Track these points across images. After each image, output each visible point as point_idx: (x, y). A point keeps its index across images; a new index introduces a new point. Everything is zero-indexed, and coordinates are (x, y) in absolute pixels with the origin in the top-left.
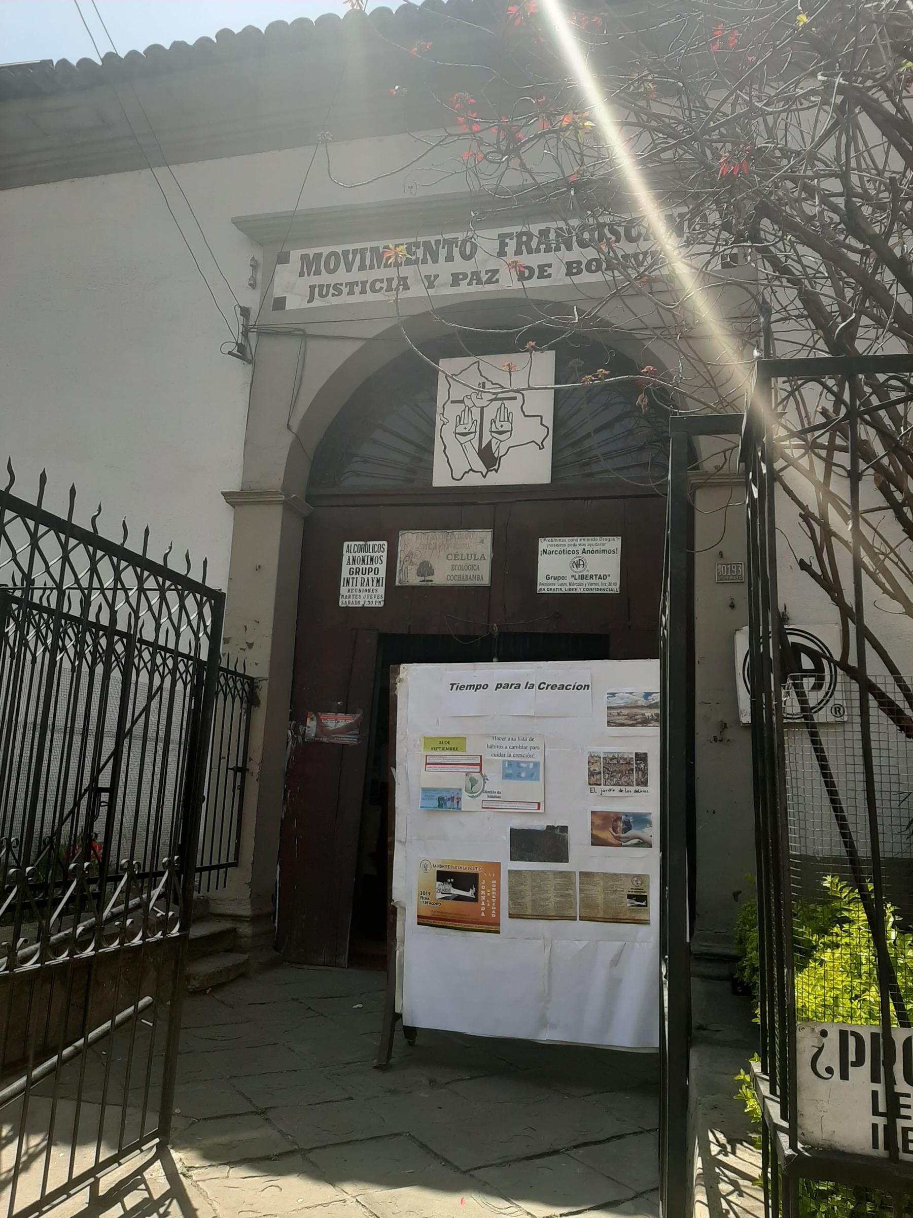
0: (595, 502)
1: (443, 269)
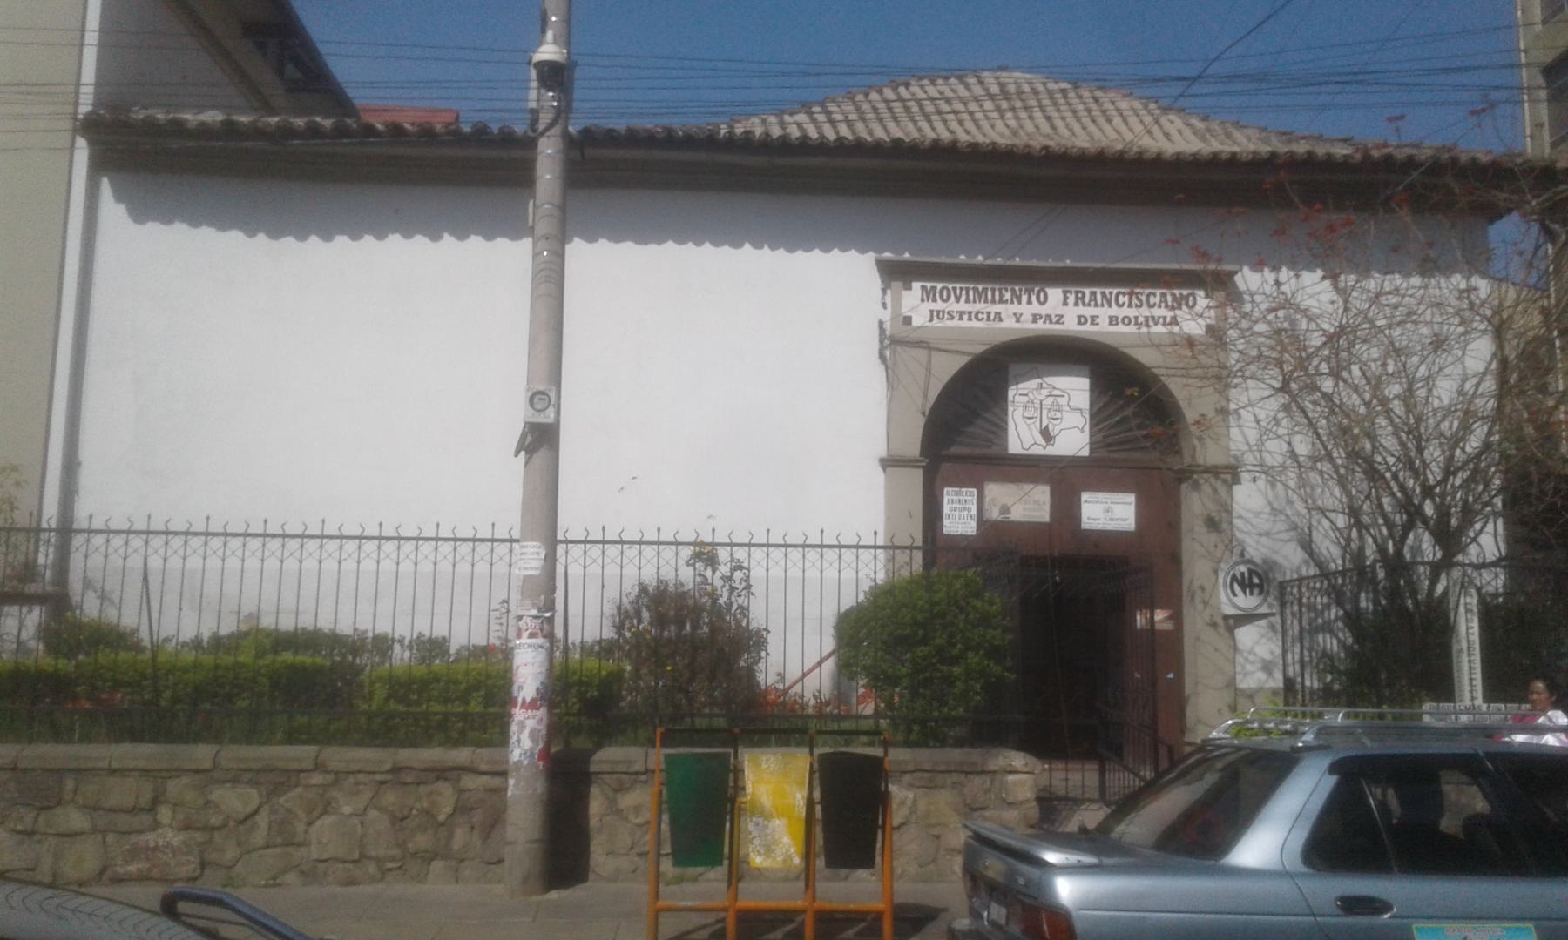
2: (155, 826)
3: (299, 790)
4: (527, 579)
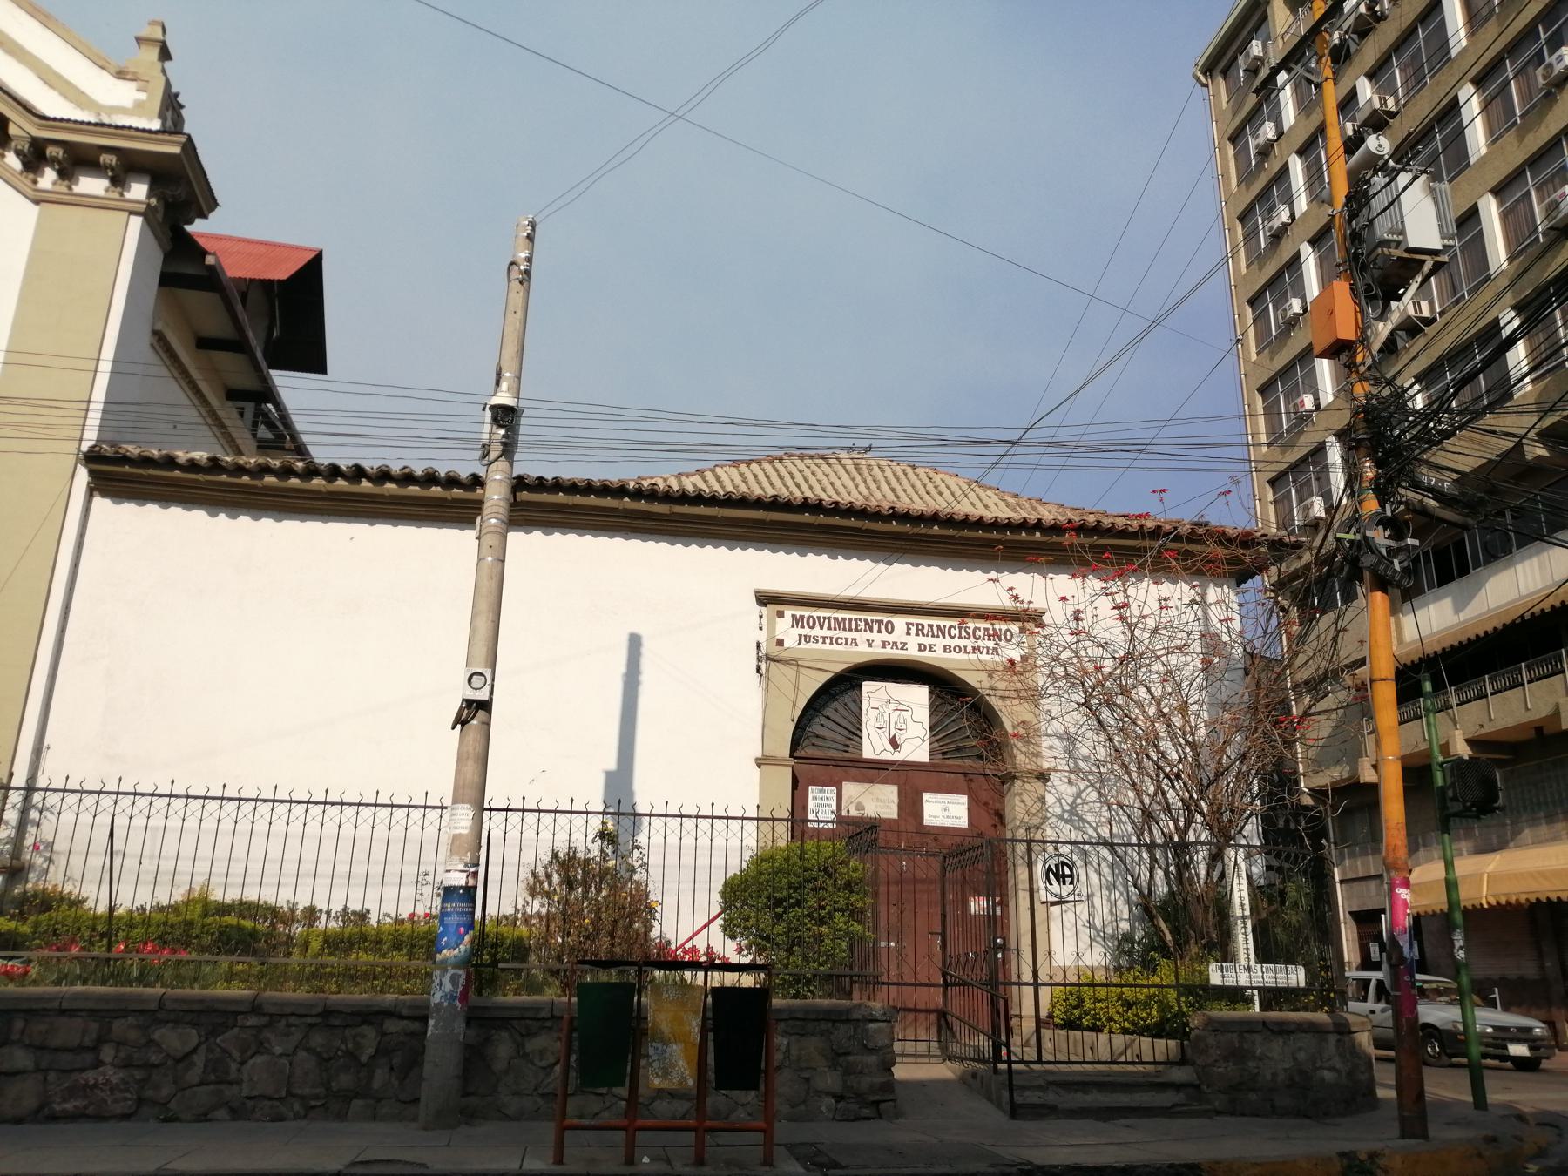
0: (952, 775)
1: (877, 638)
2: (98, 1064)
3: (236, 1030)
4: (456, 838)
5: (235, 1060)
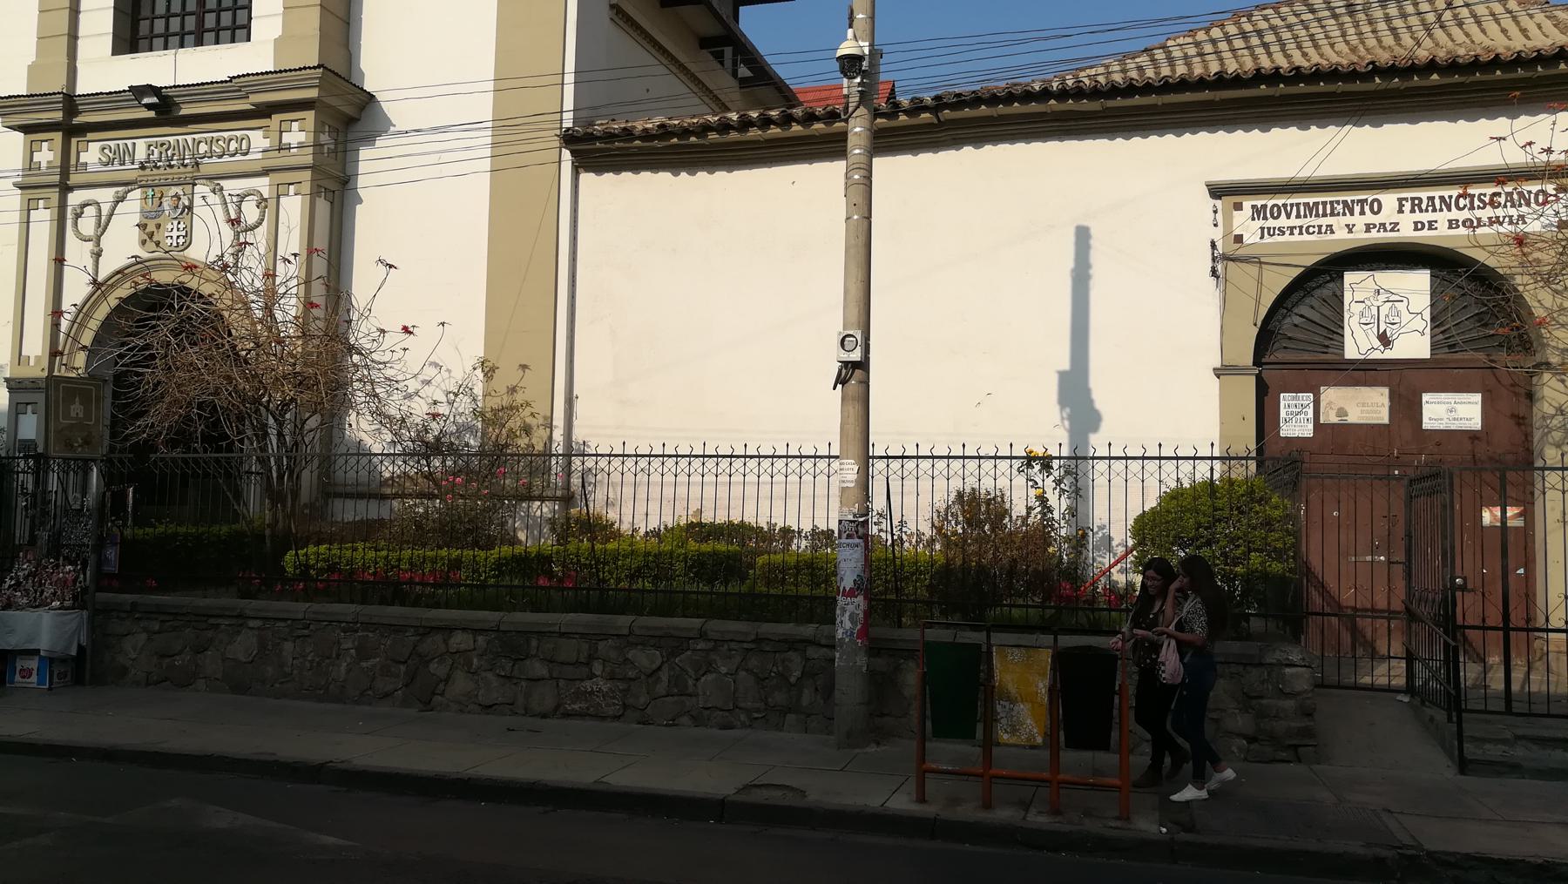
1: (1359, 221)
2: (592, 676)
3: (689, 653)
5: (691, 677)
